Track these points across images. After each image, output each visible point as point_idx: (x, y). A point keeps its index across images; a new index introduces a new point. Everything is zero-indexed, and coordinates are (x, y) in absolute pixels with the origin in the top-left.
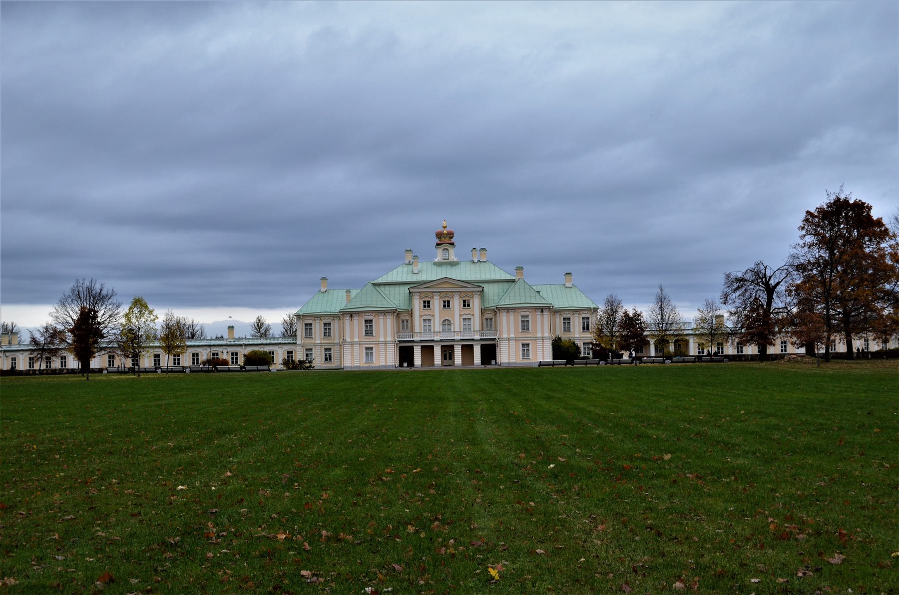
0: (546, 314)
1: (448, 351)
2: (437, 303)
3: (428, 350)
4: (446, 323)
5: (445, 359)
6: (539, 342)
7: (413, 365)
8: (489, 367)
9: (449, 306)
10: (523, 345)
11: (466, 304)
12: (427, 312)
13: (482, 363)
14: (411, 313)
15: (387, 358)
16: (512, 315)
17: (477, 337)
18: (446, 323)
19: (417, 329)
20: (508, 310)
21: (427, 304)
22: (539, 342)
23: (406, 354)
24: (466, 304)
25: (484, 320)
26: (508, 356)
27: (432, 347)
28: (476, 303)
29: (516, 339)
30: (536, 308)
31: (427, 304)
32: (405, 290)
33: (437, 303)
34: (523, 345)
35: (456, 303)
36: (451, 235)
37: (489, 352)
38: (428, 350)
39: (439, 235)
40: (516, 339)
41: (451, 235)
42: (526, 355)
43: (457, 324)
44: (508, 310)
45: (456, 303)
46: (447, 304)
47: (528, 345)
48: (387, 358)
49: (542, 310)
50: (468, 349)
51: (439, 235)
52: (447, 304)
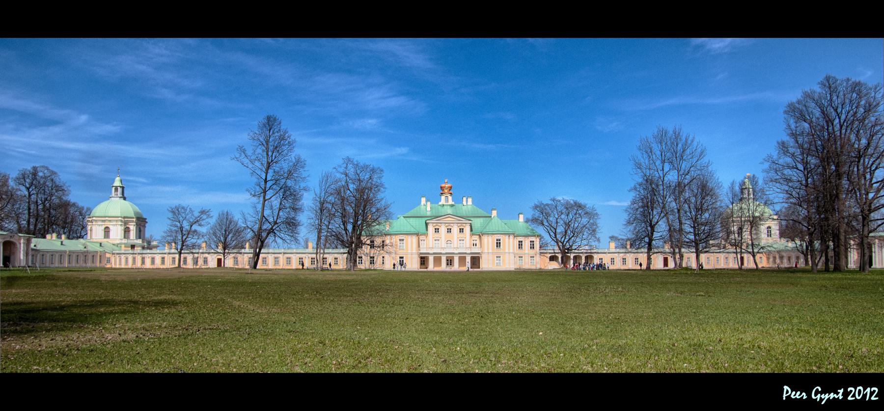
0: (512, 237)
1: (450, 262)
2: (443, 229)
3: (438, 260)
6: (507, 255)
12: (437, 235)
14: (426, 235)
15: (413, 265)
17: (469, 252)
18: (448, 241)
22: (507, 255)
23: (424, 261)
26: (486, 265)
27: (440, 258)
31: (437, 230)
33: (443, 229)
35: (455, 229)
38: (438, 260)
40: (492, 253)
46: (449, 231)
48: (413, 265)
49: (509, 235)
50: (462, 260)
52: (449, 231)
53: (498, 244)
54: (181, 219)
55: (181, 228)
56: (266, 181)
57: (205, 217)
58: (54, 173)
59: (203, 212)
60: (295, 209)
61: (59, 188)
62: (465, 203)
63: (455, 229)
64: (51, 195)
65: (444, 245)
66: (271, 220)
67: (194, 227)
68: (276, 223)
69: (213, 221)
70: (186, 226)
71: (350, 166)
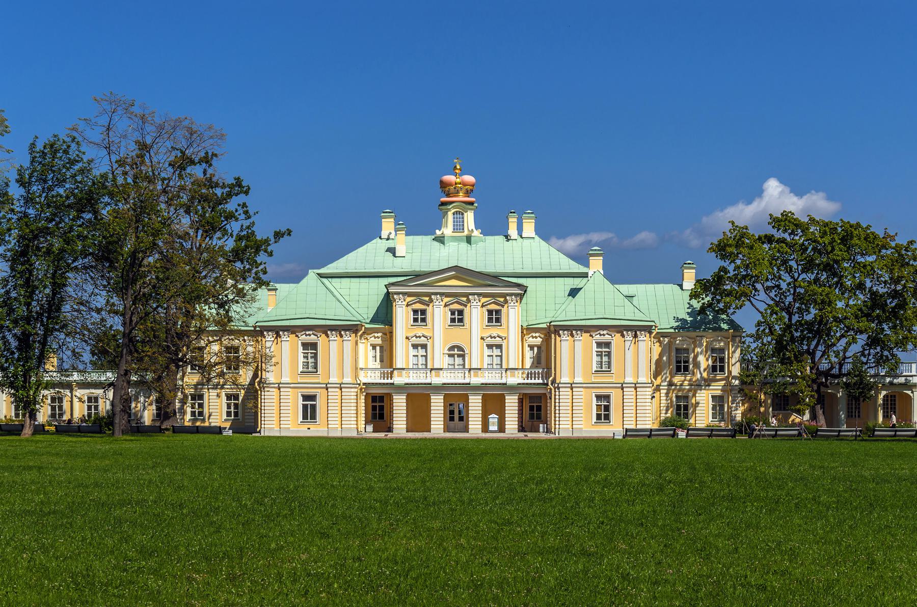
2: (439, 313)
4: (458, 352)
5: (452, 419)
7: (390, 429)
8: (531, 435)
9: (461, 320)
10: (599, 397)
11: (494, 317)
13: (522, 429)
16: (583, 339)
18: (458, 352)
19: (399, 362)
20: (571, 329)
21: (420, 317)
22: (630, 392)
23: (378, 408)
24: (494, 317)
25: (527, 349)
28: (514, 316)
29: (587, 386)
30: (621, 330)
31: (420, 317)
32: (378, 288)
33: (439, 313)
34: (599, 397)
35: (476, 314)
37: (536, 409)
40: (587, 386)
42: (604, 415)
43: (478, 355)
44: (571, 329)
45: (476, 314)
46: (458, 318)
47: (607, 398)
48: (344, 420)
52: (458, 318)
62: (513, 231)
65: (440, 358)
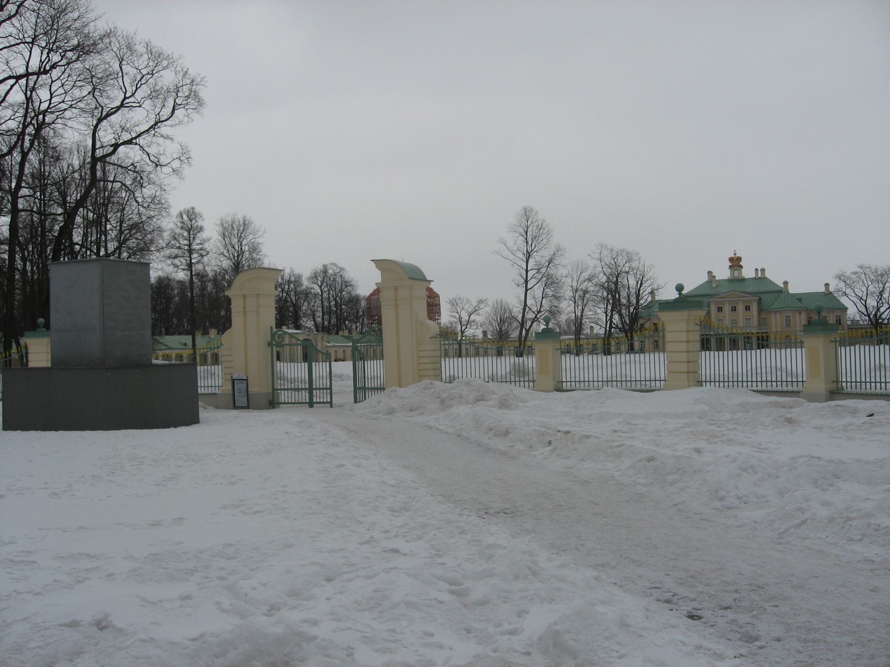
11: (747, 308)
20: (775, 312)
21: (720, 309)
24: (747, 308)
31: (720, 309)
35: (741, 308)
36: (739, 259)
39: (731, 259)
41: (739, 259)
46: (734, 309)
51: (731, 259)
52: (734, 309)
53: (788, 324)
54: (459, 310)
55: (460, 318)
56: (527, 271)
57: (482, 306)
58: (342, 269)
59: (481, 301)
60: (557, 298)
61: (347, 284)
63: (741, 308)
64: (341, 291)
66: (534, 309)
67: (473, 317)
68: (539, 312)
69: (488, 309)
70: (465, 317)
71: (605, 252)
